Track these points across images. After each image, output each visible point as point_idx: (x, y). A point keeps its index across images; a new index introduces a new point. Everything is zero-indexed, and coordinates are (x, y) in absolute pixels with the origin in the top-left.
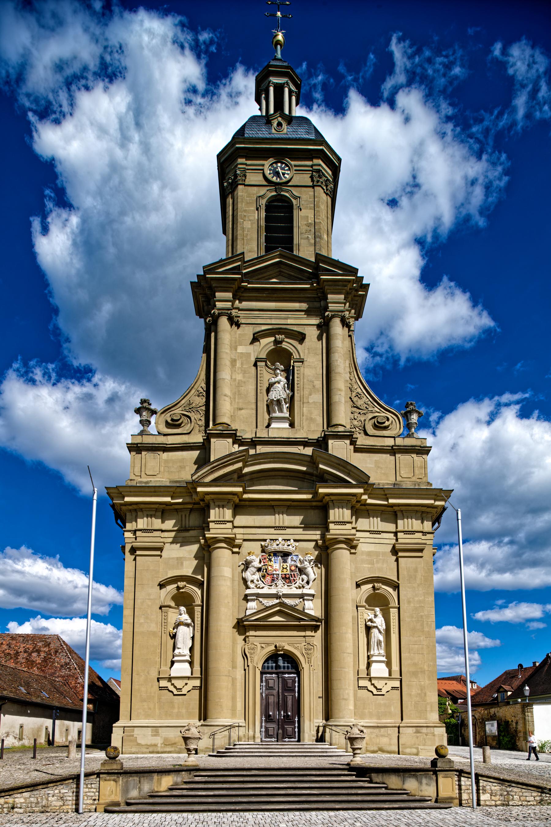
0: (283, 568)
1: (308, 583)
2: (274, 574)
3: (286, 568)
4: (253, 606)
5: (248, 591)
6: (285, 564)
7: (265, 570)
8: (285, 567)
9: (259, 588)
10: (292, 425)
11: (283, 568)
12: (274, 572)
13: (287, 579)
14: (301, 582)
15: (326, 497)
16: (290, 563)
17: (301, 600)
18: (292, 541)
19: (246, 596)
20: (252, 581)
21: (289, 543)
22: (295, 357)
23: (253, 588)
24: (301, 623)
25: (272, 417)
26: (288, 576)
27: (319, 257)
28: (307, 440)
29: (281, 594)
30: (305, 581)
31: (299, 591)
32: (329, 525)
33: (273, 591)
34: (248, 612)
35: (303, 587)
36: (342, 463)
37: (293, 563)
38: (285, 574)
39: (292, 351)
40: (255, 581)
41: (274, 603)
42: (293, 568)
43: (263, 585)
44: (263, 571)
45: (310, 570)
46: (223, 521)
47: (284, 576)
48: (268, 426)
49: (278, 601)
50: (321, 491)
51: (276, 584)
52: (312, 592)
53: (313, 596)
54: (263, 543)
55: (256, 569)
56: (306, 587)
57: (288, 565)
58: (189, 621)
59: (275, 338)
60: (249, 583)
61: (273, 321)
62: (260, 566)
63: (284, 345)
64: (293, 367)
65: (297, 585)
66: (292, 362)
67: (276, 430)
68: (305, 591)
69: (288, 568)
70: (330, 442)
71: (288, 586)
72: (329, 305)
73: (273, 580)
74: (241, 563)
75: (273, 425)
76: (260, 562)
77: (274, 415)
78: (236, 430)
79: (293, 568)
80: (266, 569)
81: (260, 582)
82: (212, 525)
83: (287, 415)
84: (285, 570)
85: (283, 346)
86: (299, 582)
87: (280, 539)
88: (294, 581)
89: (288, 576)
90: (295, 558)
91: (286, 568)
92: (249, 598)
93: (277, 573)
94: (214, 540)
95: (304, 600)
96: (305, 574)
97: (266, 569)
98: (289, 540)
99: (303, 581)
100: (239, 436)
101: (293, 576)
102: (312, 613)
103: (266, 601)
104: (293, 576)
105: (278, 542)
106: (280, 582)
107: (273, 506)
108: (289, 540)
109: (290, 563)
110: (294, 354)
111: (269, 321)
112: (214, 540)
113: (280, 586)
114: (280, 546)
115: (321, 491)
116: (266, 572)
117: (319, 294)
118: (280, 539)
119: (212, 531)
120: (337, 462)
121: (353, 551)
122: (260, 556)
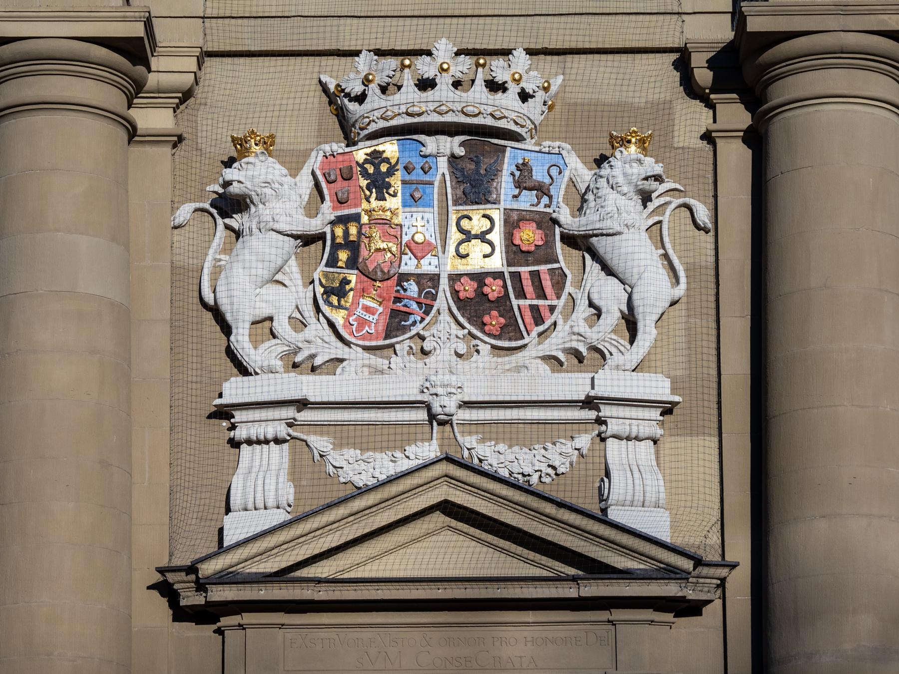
2: (403, 278)
4: (262, 485)
5: (235, 390)
7: (343, 256)
8: (477, 224)
11: (468, 236)
12: (409, 265)
13: (490, 310)
14: (583, 328)
16: (506, 202)
17: (584, 441)
18: (520, 55)
19: (223, 413)
20: (264, 325)
21: (499, 70)
26: (493, 289)
31: (575, 385)
33: (401, 378)
34: (237, 527)
37: (527, 202)
38: (479, 278)
40: (282, 326)
41: (405, 465)
42: (529, 236)
45: (635, 250)
47: (468, 288)
49: (429, 450)
52: (658, 387)
53: (668, 409)
54: (333, 74)
56: (616, 359)
57: (497, 215)
60: (241, 339)
62: (314, 225)
65: (554, 345)
68: (609, 382)
69: (496, 236)
73: (397, 322)
79: (529, 236)
81: (317, 329)
84: (477, 249)
86: (570, 329)
87: (444, 49)
88: (538, 319)
89: (493, 289)
90: (539, 175)
91: (482, 237)
92: (241, 433)
93: (428, 265)
97: (353, 247)
98: (506, 53)
102: (658, 525)
103: (352, 453)
105: (426, 67)
106: (444, 329)
108: (506, 53)
109: (506, 202)
113: (443, 356)
114: (443, 91)
116: (352, 263)
118: (444, 49)
122: (315, 161)
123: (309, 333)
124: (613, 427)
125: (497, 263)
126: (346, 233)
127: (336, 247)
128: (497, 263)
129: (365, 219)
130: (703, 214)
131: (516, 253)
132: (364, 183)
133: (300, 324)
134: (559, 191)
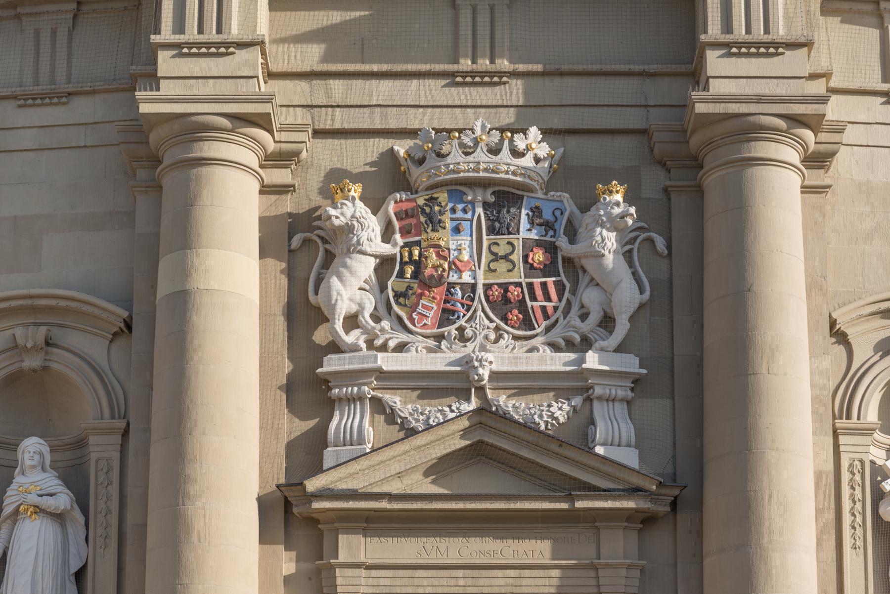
0: (496, 257)
1: (607, 322)
2: (452, 285)
3: (506, 257)
5: (331, 364)
6: (503, 239)
7: (409, 270)
8: (502, 250)
9: (384, 348)
14: (577, 322)
17: (577, 401)
23: (355, 348)
24: (579, 504)
29: (485, 373)
30: (595, 316)
32: (702, 57)
35: (586, 344)
38: (505, 287)
40: (366, 317)
43: (404, 337)
44: (401, 274)
46: (218, 45)
51: (461, 329)
52: (631, 364)
55: (372, 262)
58: (63, 500)
62: (387, 249)
71: (516, 338)
73: (447, 316)
74: (296, 240)
76: (387, 237)
79: (538, 256)
80: (411, 261)
82: (166, 63)
84: (502, 266)
91: (506, 257)
93: (467, 277)
94: (176, 126)
95: (589, 400)
96: (593, 282)
99: (584, 317)
101: (539, 292)
104: (539, 292)
112: (176, 126)
114: (481, 155)
116: (416, 275)
119: (167, 89)
121: (816, 177)
123: (386, 324)
124: (598, 391)
125: (519, 275)
126: (411, 254)
127: (403, 264)
128: (519, 275)
129: (424, 244)
130: (660, 243)
131: (530, 268)
132: (423, 219)
133: (376, 318)
134: (561, 226)
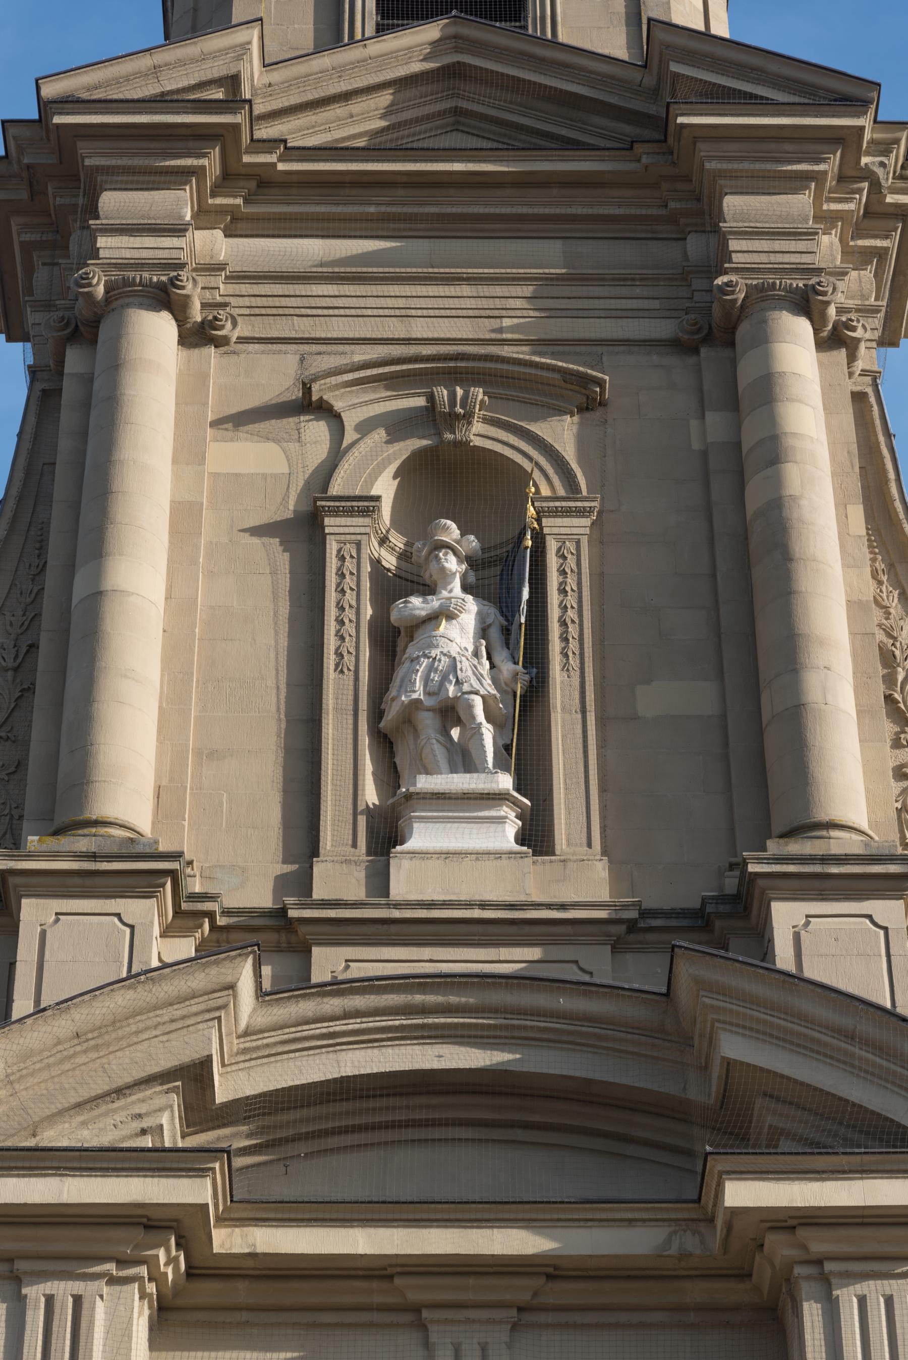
10: (536, 836)
15: (771, 1239)
22: (545, 491)
25: (409, 797)
27: (660, 35)
28: (633, 914)
36: (865, 1027)
39: (527, 466)
48: (385, 835)
50: (741, 1194)
59: (431, 398)
61: (420, 329)
63: (479, 433)
64: (539, 539)
66: (531, 511)
67: (435, 864)
70: (785, 916)
72: (733, 245)
75: (424, 836)
77: (425, 783)
78: (176, 856)
83: (505, 782)
85: (478, 442)
100: (204, 897)
107: (416, 1309)
110: (537, 475)
111: (396, 329)
115: (741, 1194)
117: (672, 205)
120: (845, 1021)
